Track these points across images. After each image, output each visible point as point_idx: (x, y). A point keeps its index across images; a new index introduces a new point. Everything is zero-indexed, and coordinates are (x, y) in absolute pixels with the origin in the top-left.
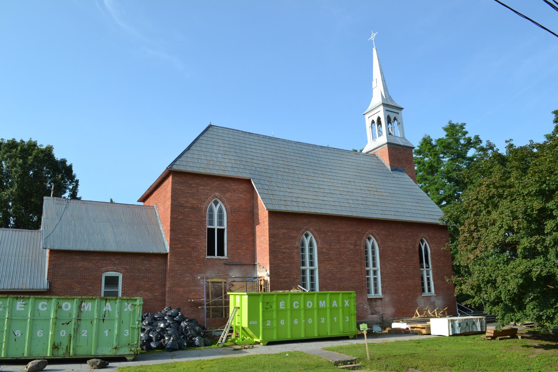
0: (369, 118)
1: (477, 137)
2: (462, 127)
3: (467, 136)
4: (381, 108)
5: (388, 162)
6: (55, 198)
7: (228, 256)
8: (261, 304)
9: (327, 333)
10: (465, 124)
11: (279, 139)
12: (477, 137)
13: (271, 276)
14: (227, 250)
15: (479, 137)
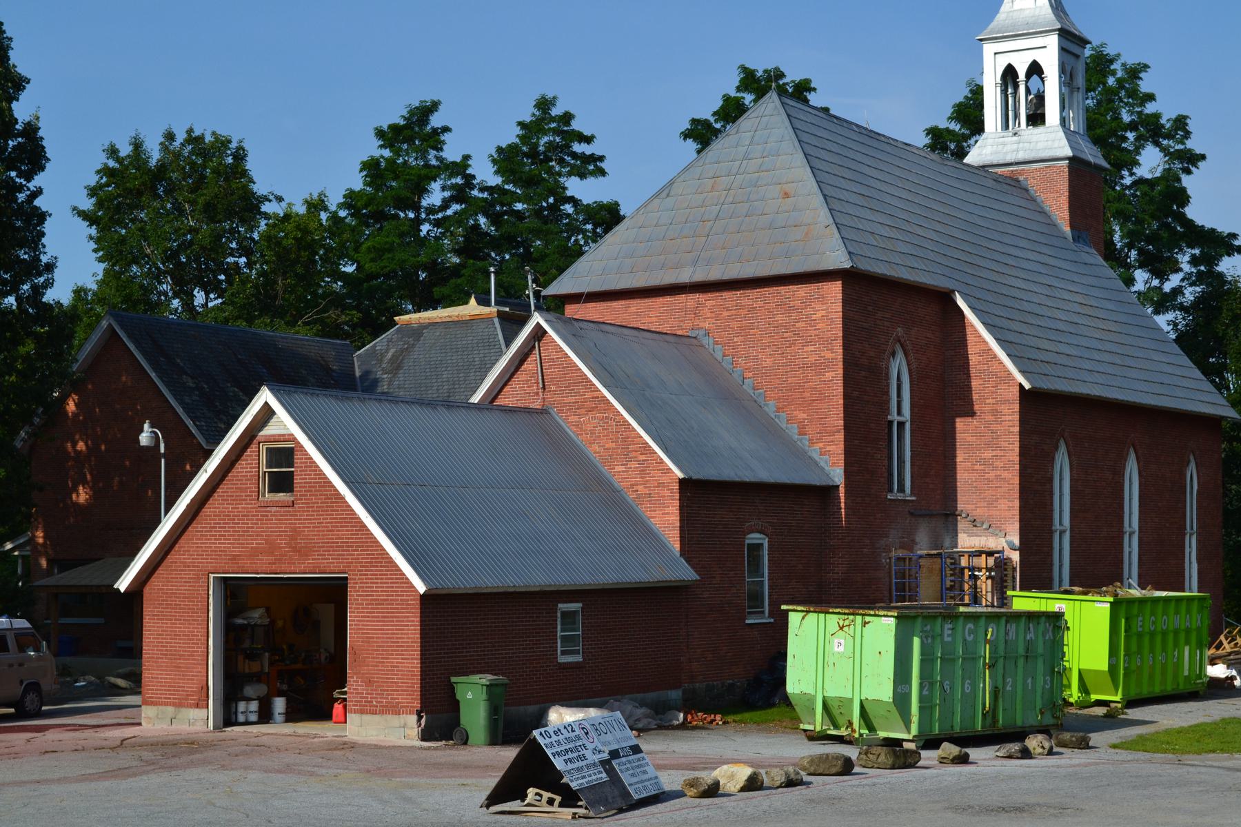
0: (995, 54)
1: (1181, 123)
2: (1134, 73)
3: (1150, 108)
4: (1053, 41)
5: (1066, 215)
6: (976, 408)
7: (912, 494)
8: (1123, 620)
9: (1178, 685)
10: (1146, 67)
11: (879, 134)
12: (1181, 123)
13: (1023, 548)
14: (912, 477)
15: (1188, 121)
